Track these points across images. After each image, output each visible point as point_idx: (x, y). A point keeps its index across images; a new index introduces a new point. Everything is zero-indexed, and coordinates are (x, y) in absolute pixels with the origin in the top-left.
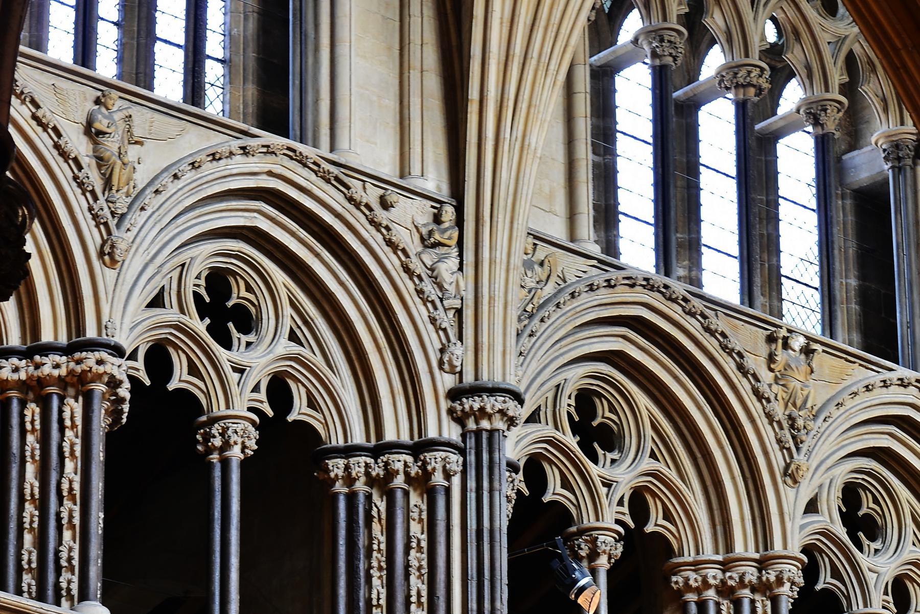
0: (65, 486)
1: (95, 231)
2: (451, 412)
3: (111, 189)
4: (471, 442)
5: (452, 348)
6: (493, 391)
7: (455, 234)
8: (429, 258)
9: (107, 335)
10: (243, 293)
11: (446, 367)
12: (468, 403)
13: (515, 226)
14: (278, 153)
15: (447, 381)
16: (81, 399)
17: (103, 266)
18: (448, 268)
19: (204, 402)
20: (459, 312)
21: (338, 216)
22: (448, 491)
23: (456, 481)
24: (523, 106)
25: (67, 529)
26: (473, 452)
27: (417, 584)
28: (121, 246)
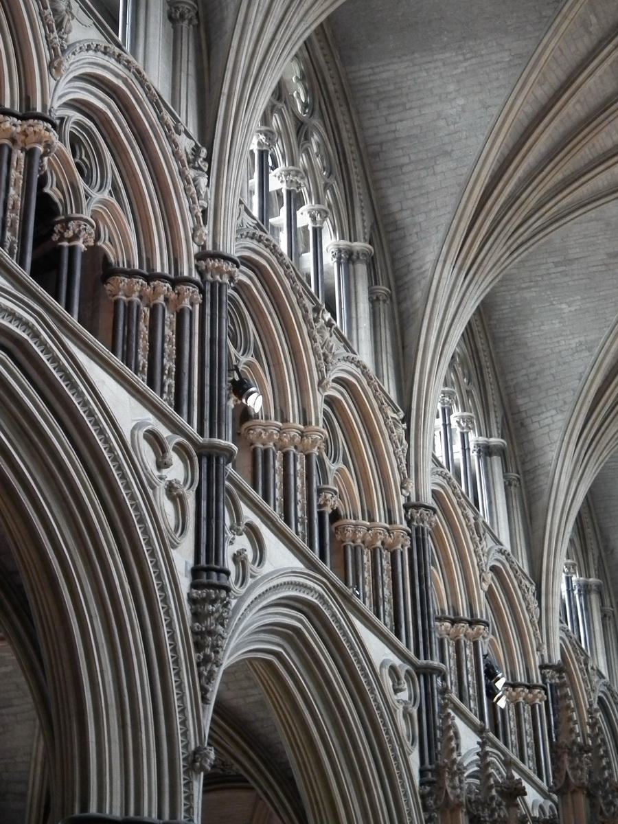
0: (11, 202)
1: (47, 52)
2: (197, 267)
3: (61, 30)
4: (208, 287)
5: (203, 227)
6: (227, 259)
7: (207, 165)
8: (191, 173)
9: (50, 115)
10: (83, 157)
11: (197, 239)
12: (210, 263)
13: (240, 172)
14: (132, 70)
15: (195, 249)
16: (24, 153)
17: (50, 77)
18: (203, 181)
19: (61, 209)
20: (204, 212)
21: (152, 126)
22: (191, 314)
23: (197, 307)
24: (251, 105)
25: (9, 231)
26: (209, 293)
27: (170, 364)
28: (66, 64)
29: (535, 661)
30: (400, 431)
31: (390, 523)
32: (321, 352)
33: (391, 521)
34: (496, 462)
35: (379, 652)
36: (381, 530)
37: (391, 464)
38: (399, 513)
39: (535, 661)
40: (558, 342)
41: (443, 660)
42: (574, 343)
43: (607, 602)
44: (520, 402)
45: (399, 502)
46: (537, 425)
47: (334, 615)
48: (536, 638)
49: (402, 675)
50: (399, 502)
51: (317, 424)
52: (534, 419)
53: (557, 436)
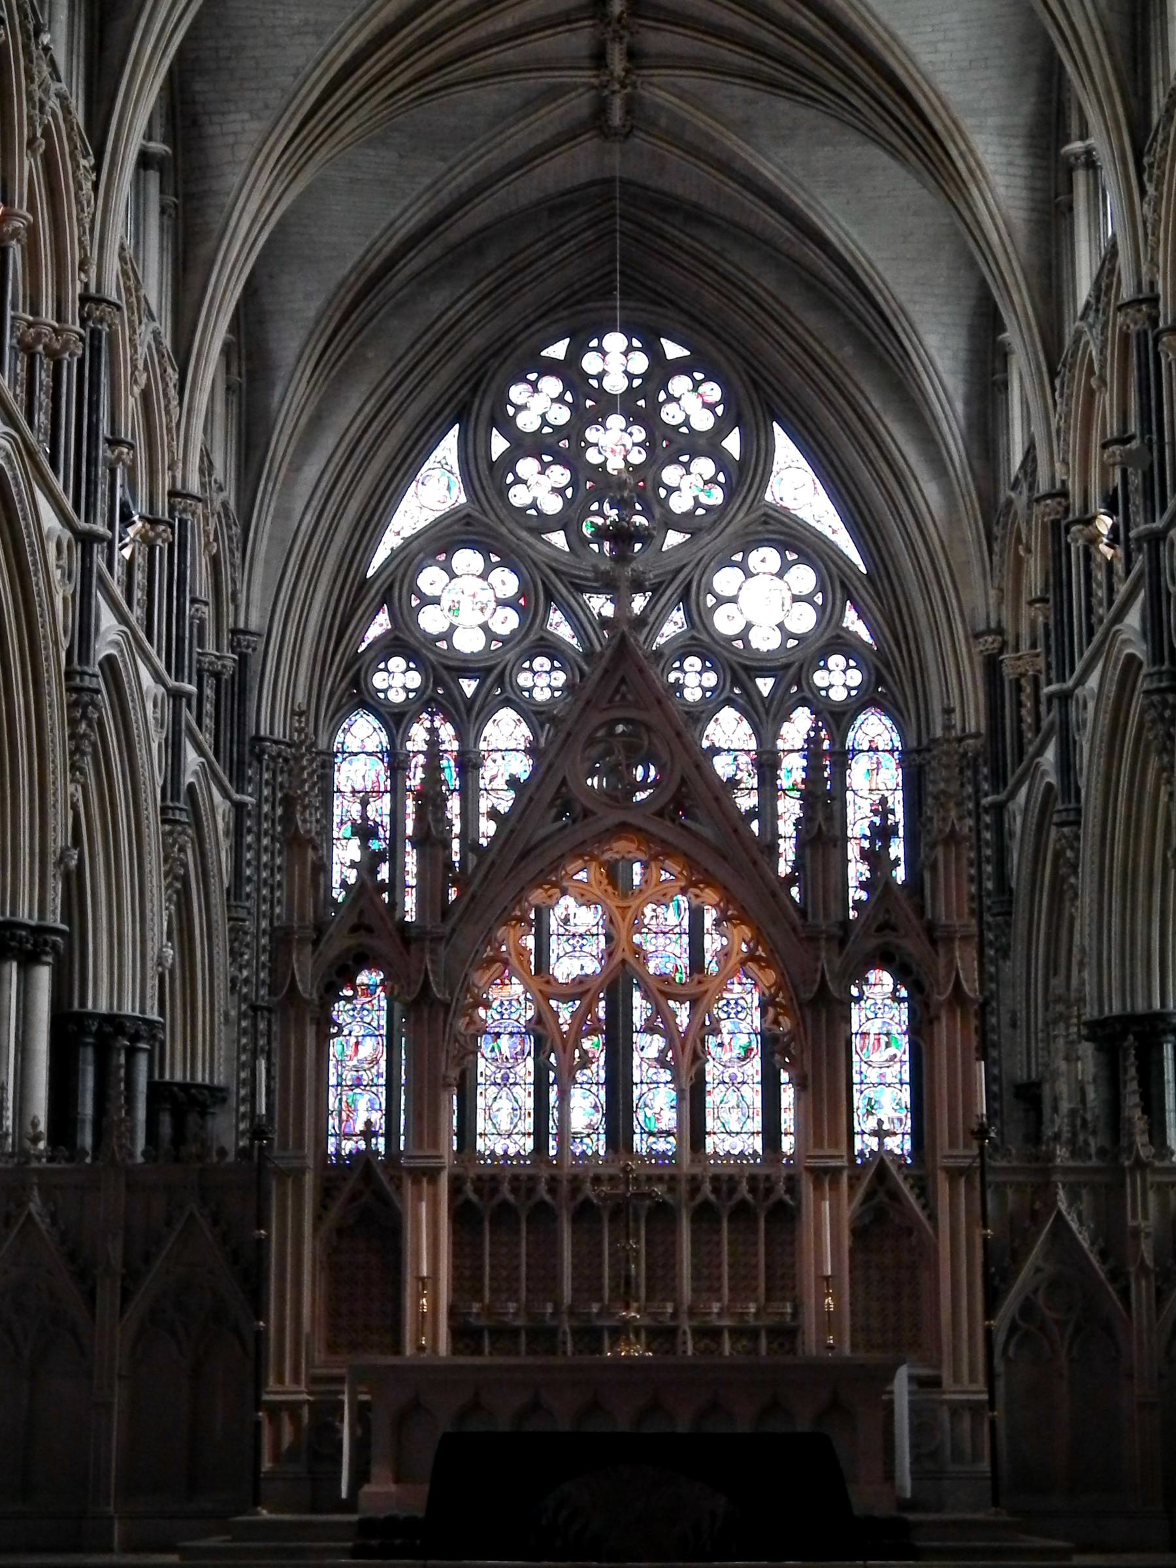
29: (164, 483)
30: (87, 186)
31: (59, 320)
32: (38, 94)
33: (60, 316)
34: (153, 177)
35: (49, 519)
36: (46, 330)
37: (72, 232)
38: (73, 308)
39: (164, 483)
40: (274, 12)
41: (111, 527)
42: (297, 18)
43: (234, 369)
44: (198, 87)
45: (75, 289)
46: (217, 129)
47: (15, 478)
48: (171, 451)
49: (65, 544)
50: (75, 289)
51: (21, 206)
52: (216, 119)
53: (245, 153)
